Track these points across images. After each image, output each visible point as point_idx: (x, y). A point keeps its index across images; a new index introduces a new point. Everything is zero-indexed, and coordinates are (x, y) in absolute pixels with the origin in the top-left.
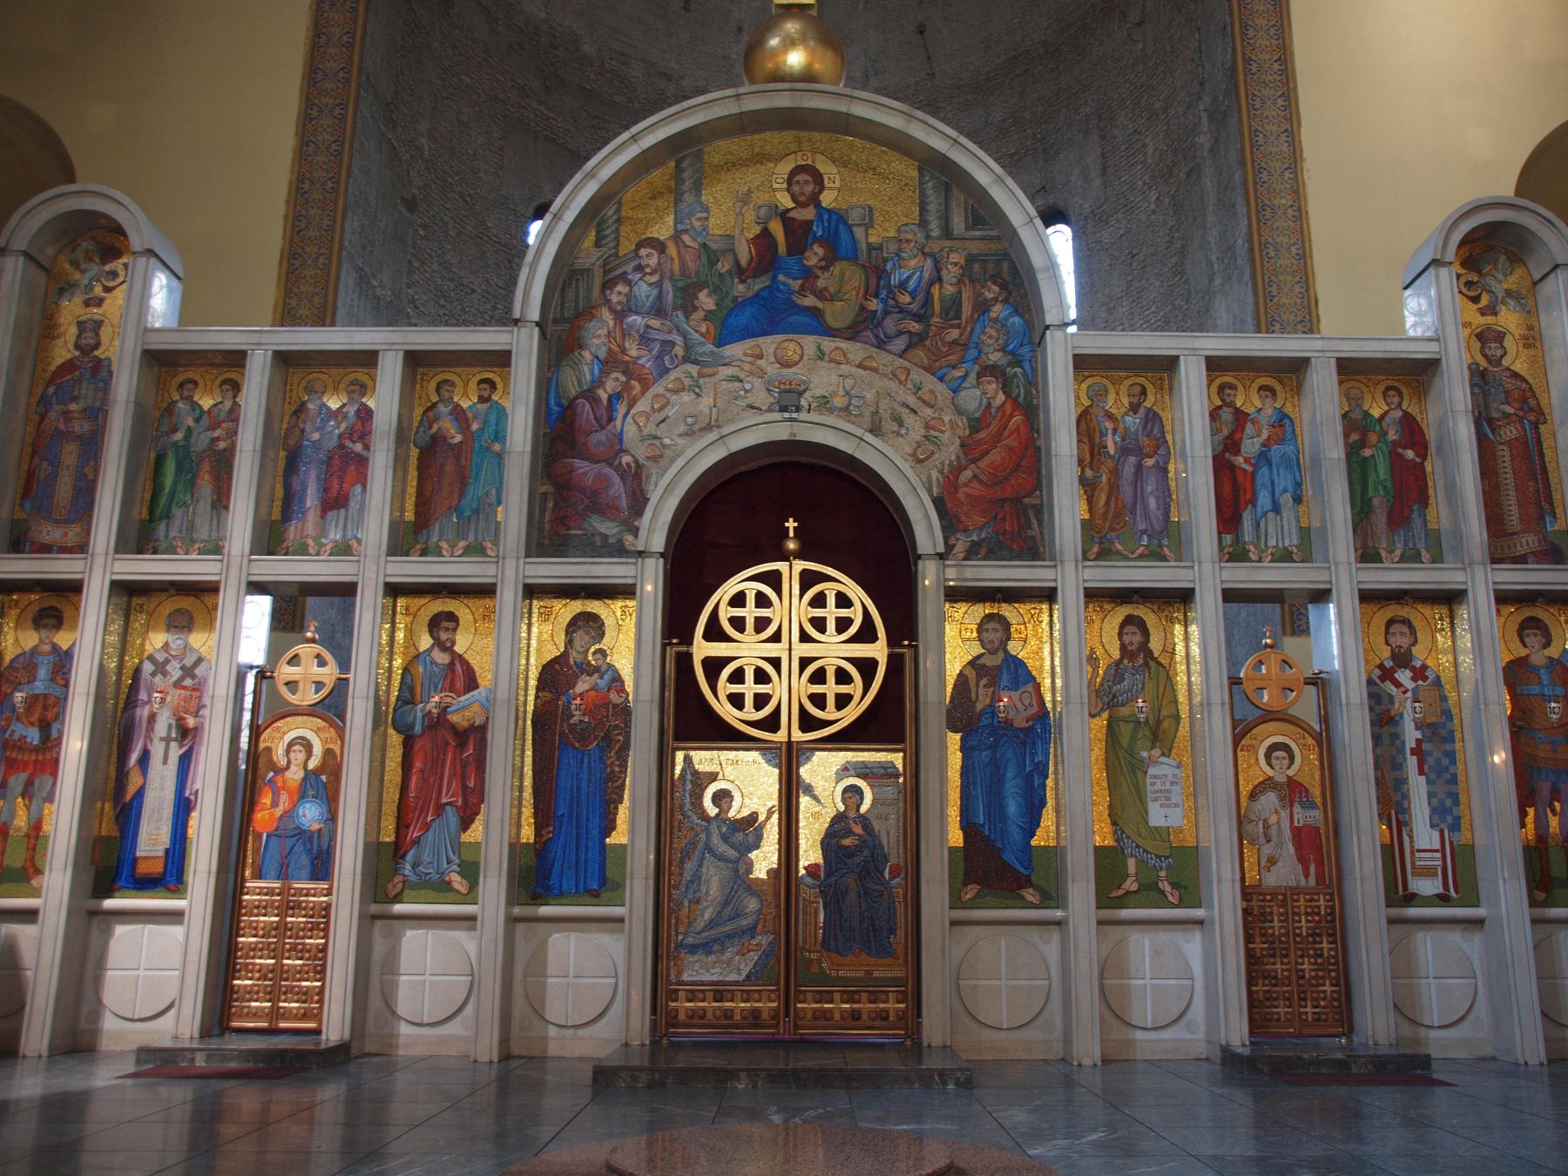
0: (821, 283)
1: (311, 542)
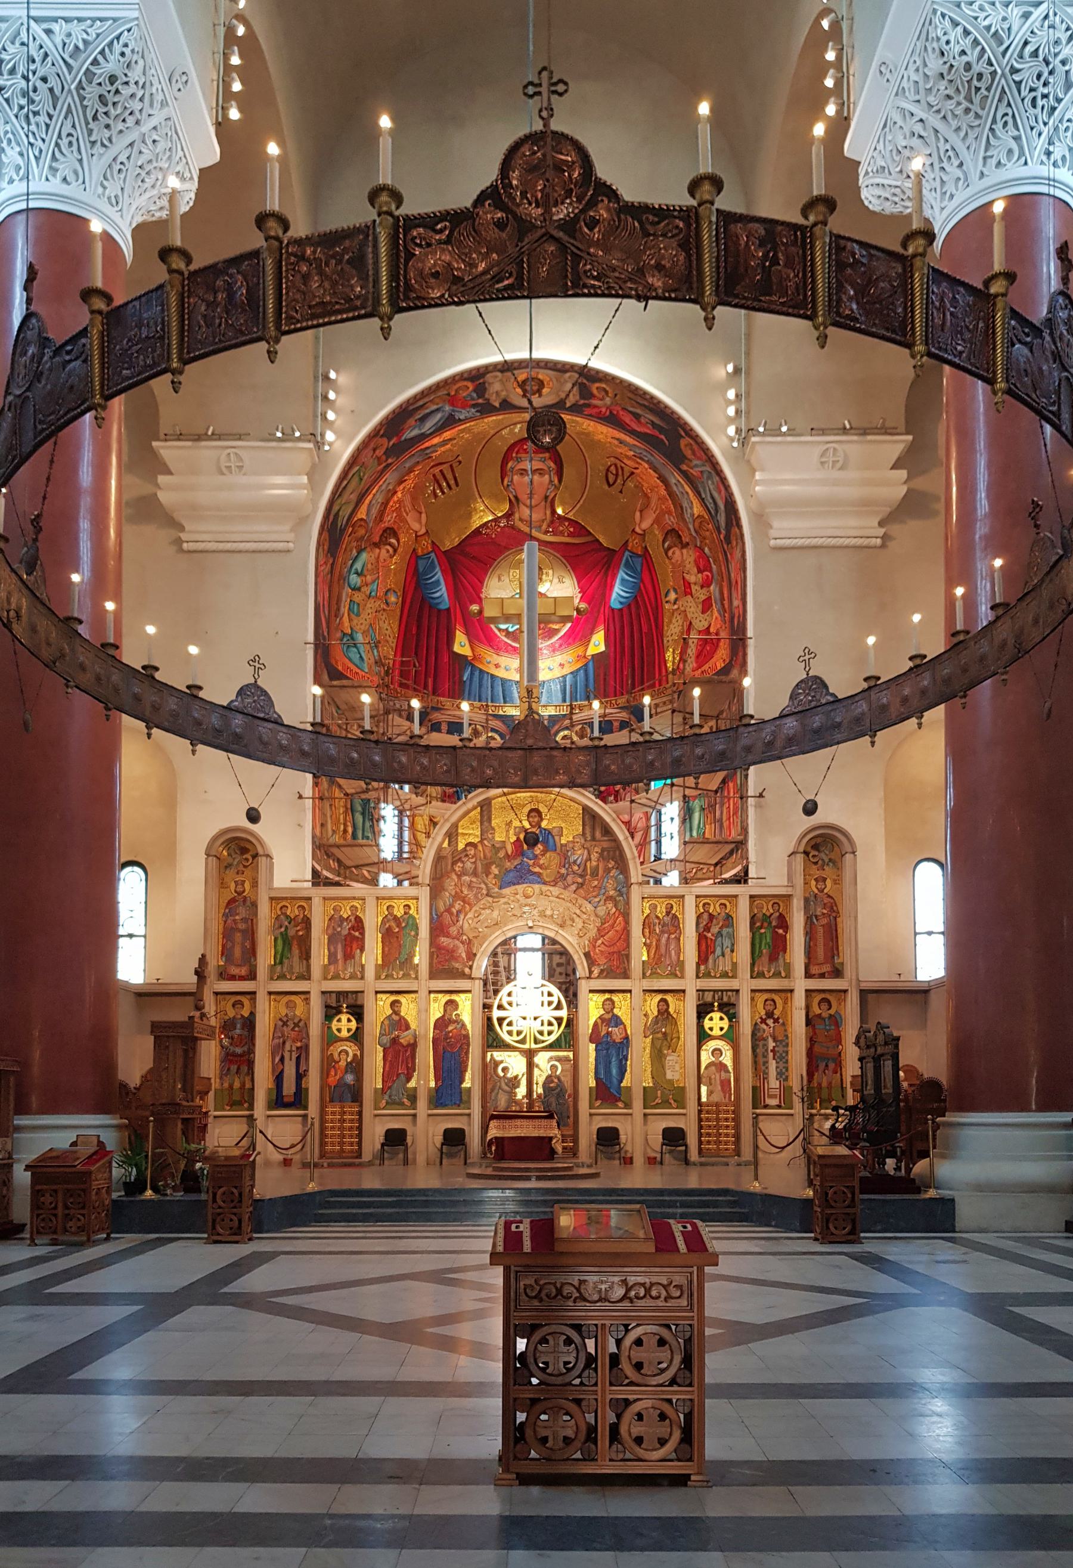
0: (541, 862)
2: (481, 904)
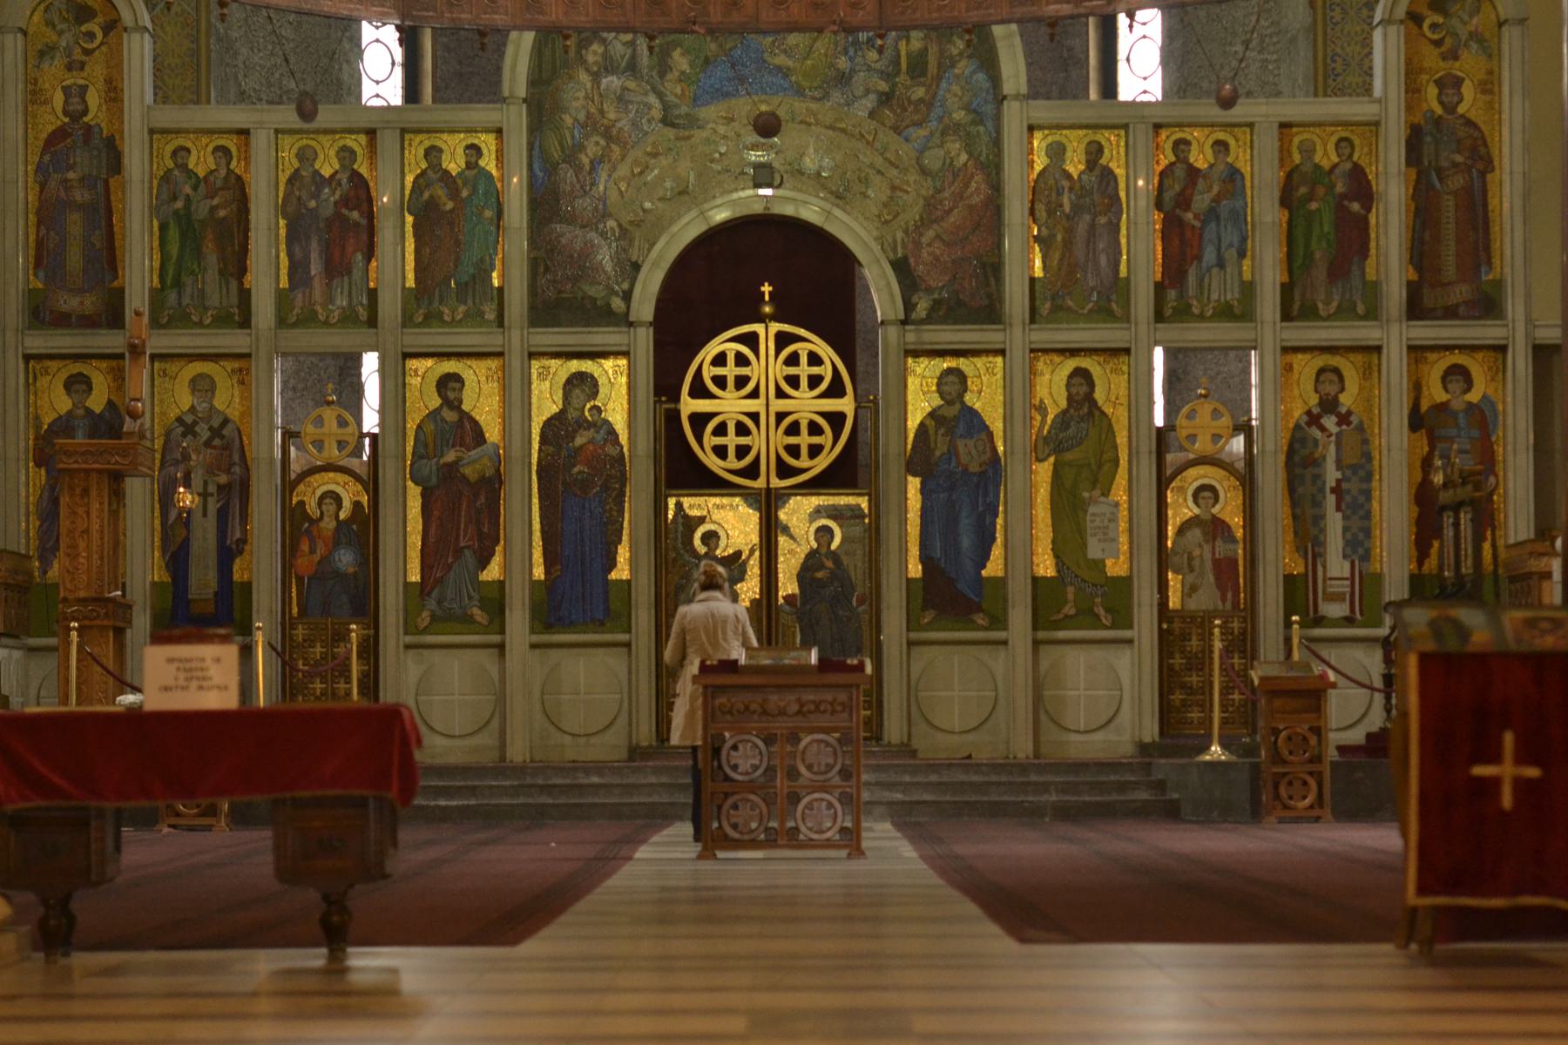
1: (318, 308)
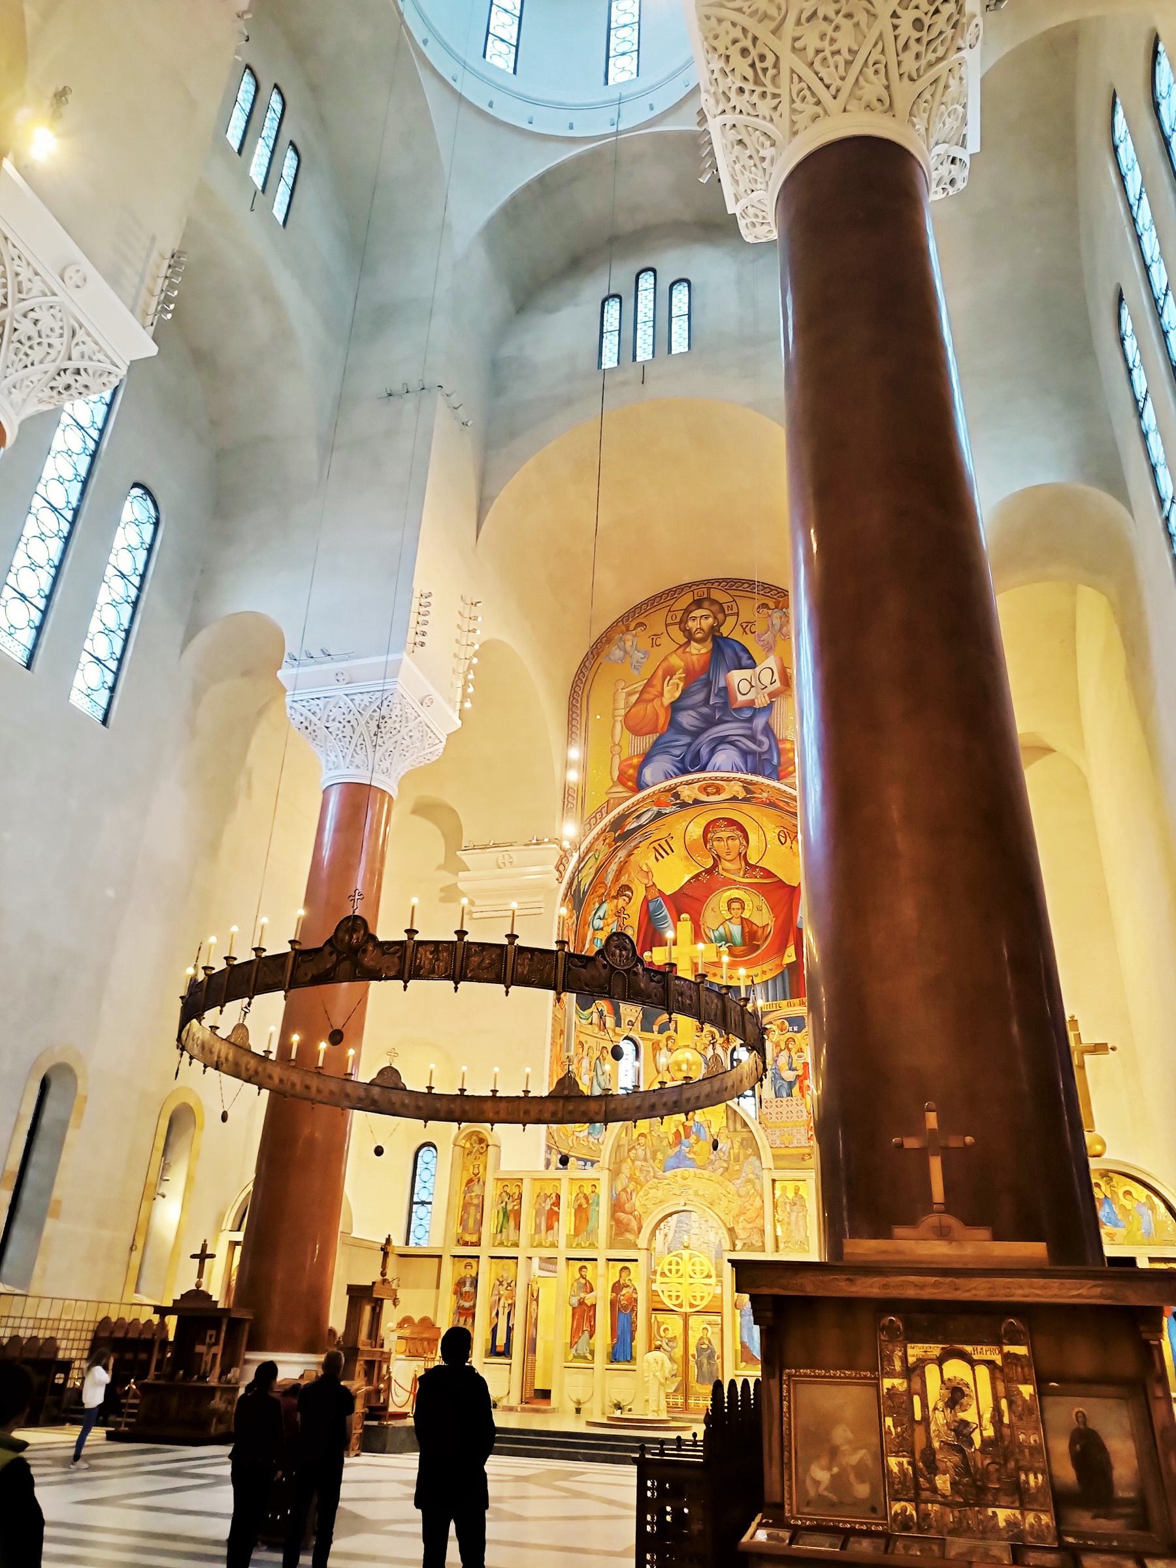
2: (649, 1185)
